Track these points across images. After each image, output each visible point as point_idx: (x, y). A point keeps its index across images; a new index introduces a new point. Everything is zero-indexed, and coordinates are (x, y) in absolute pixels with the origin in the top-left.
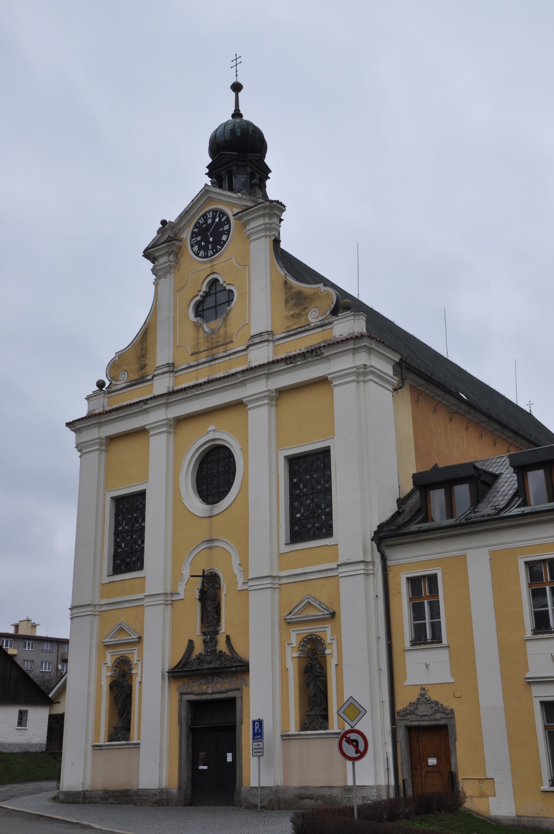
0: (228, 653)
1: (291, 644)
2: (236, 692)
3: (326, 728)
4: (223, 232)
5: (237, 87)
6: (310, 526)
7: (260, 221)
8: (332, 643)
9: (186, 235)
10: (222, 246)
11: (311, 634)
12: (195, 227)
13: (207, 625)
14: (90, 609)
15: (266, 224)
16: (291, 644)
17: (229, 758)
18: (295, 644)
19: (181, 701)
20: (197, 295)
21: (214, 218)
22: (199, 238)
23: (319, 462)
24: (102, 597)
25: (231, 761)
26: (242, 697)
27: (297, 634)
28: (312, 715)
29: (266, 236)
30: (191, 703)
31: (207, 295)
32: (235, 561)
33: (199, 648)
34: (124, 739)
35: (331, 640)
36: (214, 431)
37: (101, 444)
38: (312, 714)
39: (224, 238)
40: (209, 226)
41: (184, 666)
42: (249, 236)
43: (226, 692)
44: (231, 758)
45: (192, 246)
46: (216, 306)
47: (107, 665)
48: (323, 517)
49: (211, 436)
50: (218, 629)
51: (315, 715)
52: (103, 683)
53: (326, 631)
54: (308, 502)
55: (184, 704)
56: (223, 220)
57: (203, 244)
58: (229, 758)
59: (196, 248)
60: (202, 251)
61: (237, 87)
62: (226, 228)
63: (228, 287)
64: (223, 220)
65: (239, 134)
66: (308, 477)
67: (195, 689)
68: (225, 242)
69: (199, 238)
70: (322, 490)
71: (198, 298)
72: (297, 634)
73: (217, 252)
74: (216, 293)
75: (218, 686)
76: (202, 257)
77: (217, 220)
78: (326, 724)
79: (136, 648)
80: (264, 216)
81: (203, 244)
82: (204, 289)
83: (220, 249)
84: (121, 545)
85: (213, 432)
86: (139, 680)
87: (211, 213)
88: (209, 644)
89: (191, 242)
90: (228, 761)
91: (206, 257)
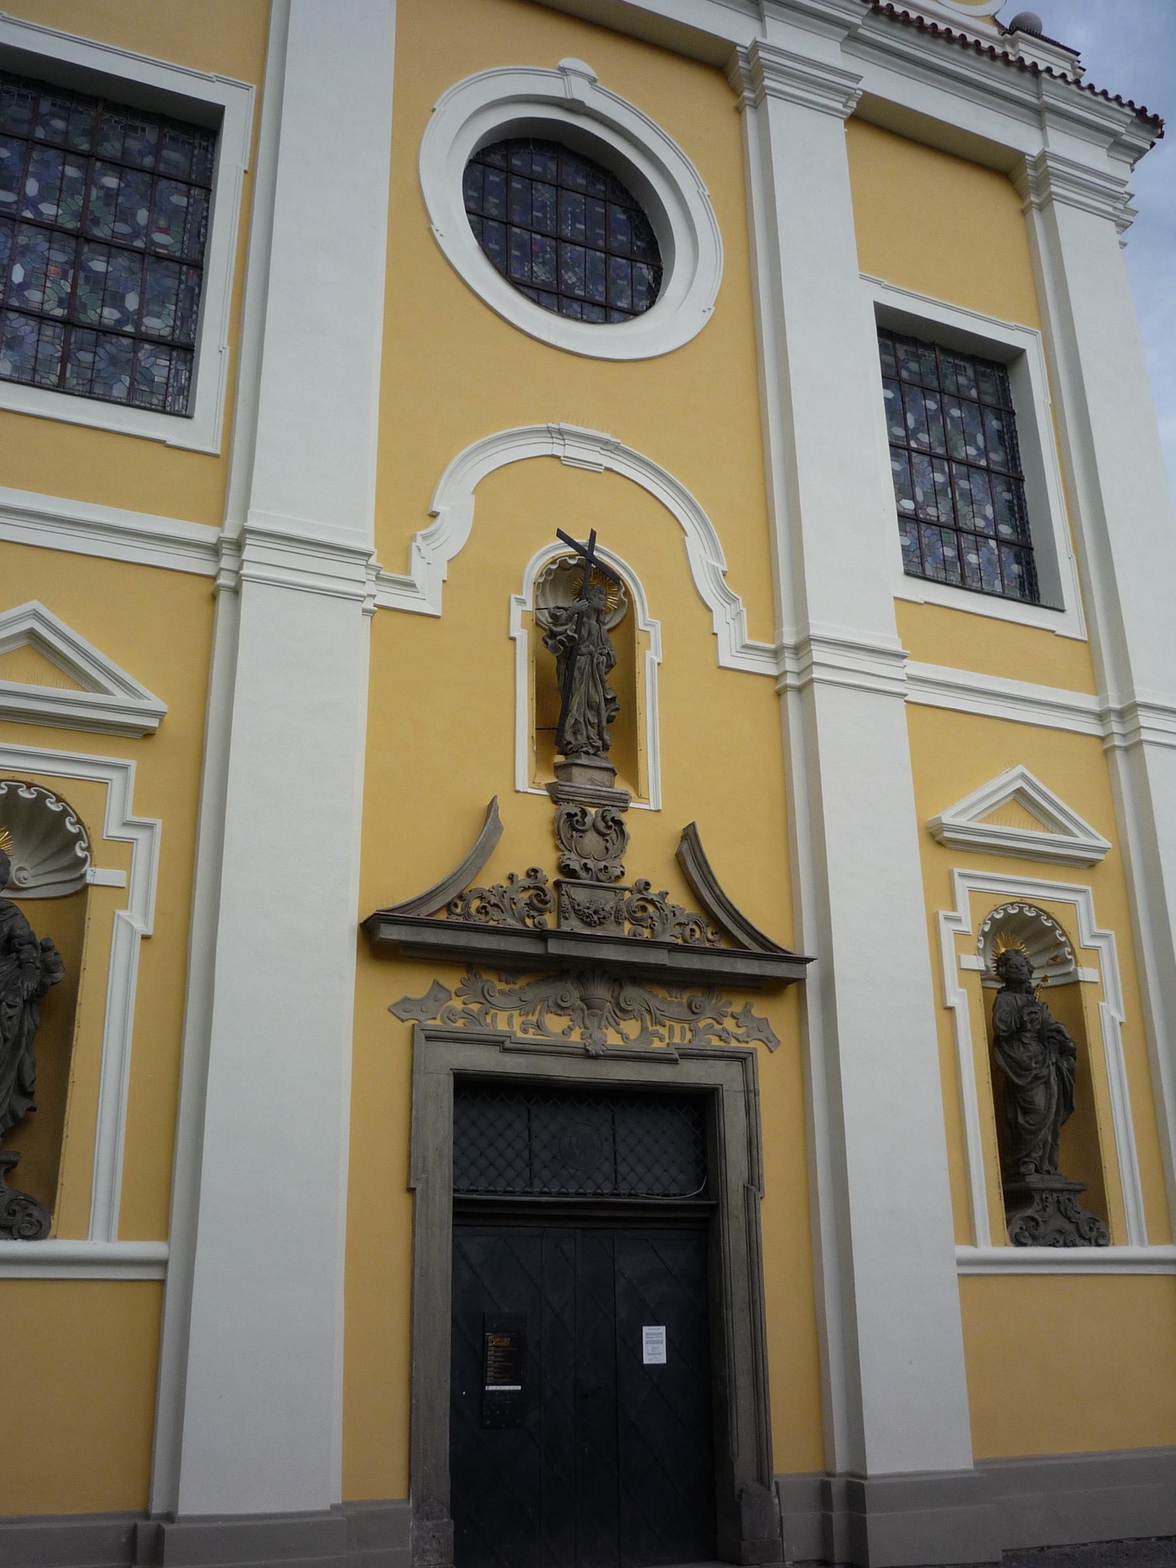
0: (678, 898)
1: (958, 920)
2: (721, 1064)
3: (1100, 1239)
8: (1096, 949)
11: (1021, 903)
13: (559, 759)
16: (958, 920)
17: (654, 1346)
18: (966, 926)
25: (662, 1359)
26: (750, 1094)
27: (972, 891)
28: (1052, 1190)
32: (704, 560)
33: (529, 845)
35: (1094, 936)
38: (1059, 1186)
41: (449, 907)
43: (674, 1062)
44: (662, 1348)
48: (993, 543)
51: (1061, 1191)
53: (1073, 904)
58: (654, 1346)
66: (932, 405)
67: (506, 1022)
72: (972, 891)
75: (632, 1028)
78: (1101, 1225)
79: (133, 764)
88: (591, 841)
90: (647, 1360)
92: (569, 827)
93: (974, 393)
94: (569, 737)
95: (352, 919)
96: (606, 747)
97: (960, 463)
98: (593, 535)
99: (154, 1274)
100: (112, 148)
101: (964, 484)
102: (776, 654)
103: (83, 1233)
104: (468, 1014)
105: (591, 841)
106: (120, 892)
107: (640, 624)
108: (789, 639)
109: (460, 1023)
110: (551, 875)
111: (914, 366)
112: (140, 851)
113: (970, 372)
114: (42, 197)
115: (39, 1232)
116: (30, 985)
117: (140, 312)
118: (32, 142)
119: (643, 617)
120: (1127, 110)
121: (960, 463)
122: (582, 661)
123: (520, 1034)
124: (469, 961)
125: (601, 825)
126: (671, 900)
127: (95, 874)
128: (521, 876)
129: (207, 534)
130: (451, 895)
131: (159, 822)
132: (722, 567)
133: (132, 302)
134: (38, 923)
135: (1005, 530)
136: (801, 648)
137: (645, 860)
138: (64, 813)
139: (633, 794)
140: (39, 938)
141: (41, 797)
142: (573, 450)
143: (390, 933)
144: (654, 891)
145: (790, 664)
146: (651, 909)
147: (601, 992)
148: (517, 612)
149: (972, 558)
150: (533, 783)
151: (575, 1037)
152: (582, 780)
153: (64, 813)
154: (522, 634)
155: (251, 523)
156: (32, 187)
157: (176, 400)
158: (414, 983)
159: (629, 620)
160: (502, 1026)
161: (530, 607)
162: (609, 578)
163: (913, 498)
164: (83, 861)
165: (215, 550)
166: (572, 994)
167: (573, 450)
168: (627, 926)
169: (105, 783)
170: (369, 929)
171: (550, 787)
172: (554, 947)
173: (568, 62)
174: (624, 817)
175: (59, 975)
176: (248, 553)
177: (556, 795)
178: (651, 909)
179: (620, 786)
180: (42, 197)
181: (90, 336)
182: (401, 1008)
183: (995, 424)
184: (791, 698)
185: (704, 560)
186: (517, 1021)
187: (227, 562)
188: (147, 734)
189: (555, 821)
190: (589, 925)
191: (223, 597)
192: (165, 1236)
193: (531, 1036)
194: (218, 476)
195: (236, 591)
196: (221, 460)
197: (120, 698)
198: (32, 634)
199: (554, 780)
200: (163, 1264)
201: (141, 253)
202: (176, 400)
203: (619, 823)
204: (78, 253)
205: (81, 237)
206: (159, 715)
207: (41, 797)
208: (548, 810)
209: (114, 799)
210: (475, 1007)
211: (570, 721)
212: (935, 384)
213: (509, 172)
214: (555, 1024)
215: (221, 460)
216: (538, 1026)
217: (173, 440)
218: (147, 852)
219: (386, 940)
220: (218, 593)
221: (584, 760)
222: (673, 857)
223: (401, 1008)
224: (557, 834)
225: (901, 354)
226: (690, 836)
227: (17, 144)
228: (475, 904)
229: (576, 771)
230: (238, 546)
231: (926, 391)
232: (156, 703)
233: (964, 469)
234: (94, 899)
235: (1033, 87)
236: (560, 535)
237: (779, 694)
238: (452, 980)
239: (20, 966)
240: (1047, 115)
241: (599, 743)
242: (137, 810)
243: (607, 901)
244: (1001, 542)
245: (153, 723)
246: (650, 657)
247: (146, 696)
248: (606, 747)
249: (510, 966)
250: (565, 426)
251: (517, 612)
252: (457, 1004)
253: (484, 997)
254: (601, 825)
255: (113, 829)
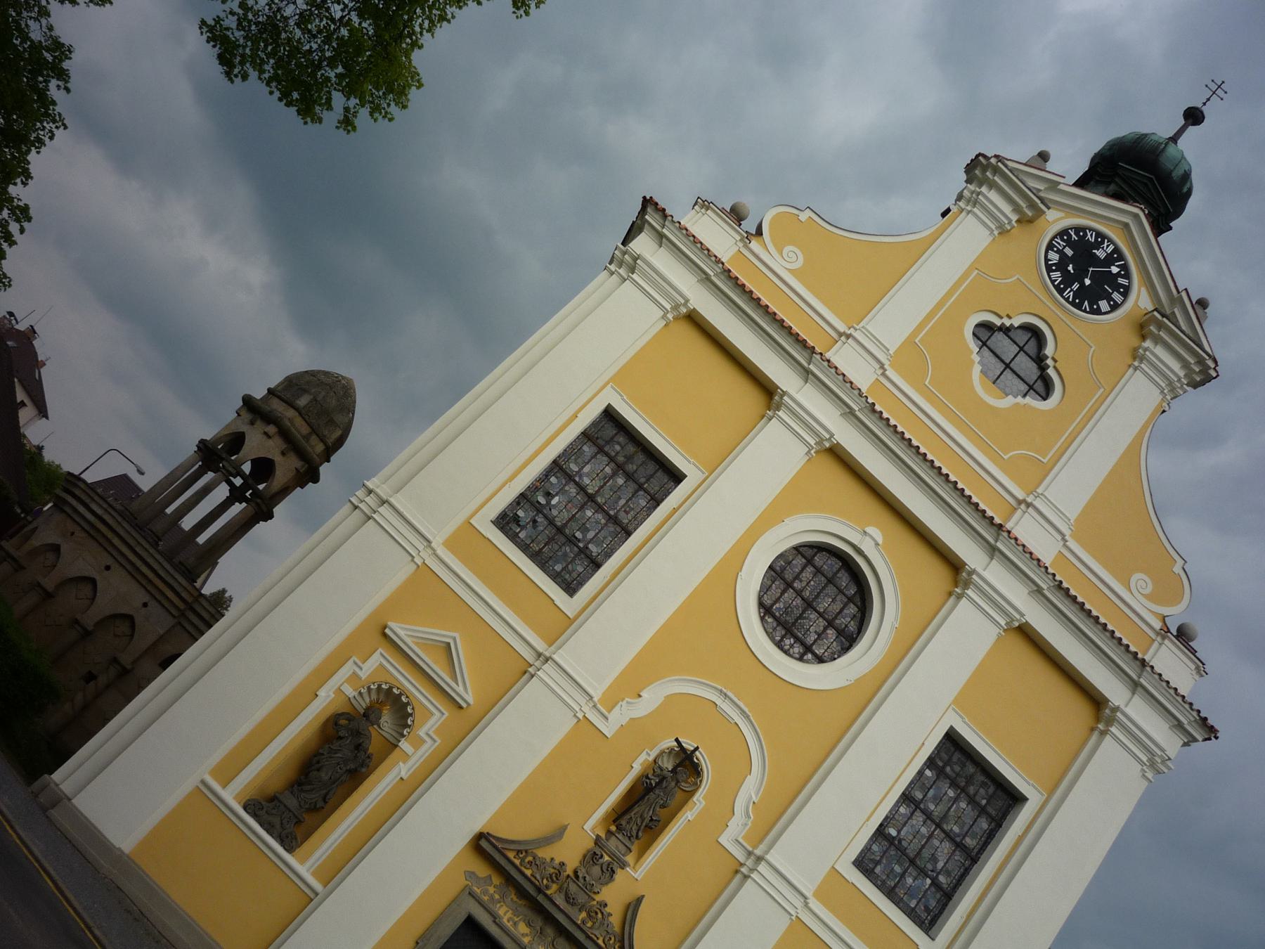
0: (615, 920)
4: (1109, 299)
5: (1194, 116)
6: (898, 869)
7: (1175, 365)
9: (1056, 221)
10: (1093, 312)
12: (1078, 229)
13: (613, 828)
14: (421, 548)
15: (1179, 380)
19: (455, 900)
20: (1001, 318)
21: (1109, 260)
22: (1069, 252)
23: (982, 791)
24: (450, 544)
29: (1162, 392)
30: (470, 923)
31: (1006, 330)
32: (750, 789)
33: (569, 853)
34: (282, 842)
36: (877, 544)
37: (676, 307)
39: (1104, 305)
40: (1096, 261)
41: (519, 852)
42: (1142, 359)
45: (1050, 247)
46: (1007, 366)
47: (357, 670)
48: (928, 881)
49: (867, 547)
50: (630, 859)
52: (322, 693)
54: (924, 830)
55: (461, 918)
56: (1121, 281)
57: (1070, 268)
59: (1054, 257)
60: (1058, 274)
61: (1194, 116)
62: (1116, 296)
63: (1051, 372)
64: (1121, 281)
65: (1185, 190)
68: (1098, 312)
69: (1069, 252)
70: (958, 839)
71: (998, 322)
73: (1079, 307)
74: (1021, 349)
76: (1053, 282)
77: (1115, 270)
79: (447, 714)
80: (1185, 365)
81: (1070, 268)
82: (1017, 322)
83: (1085, 311)
84: (553, 497)
85: (871, 541)
86: (403, 774)
87: (1111, 248)
88: (596, 870)
89: (1053, 239)
91: (1061, 292)
92: (592, 857)
93: (984, 802)
94: (624, 823)
95: (477, 827)
96: (637, 837)
97: (943, 831)
98: (697, 749)
99: (312, 896)
100: (631, 467)
101: (936, 843)
102: (750, 853)
103: (302, 862)
104: (492, 897)
105: (596, 870)
106: (406, 757)
107: (695, 799)
108: (758, 852)
109: (486, 898)
110: (569, 871)
111: (957, 768)
112: (425, 747)
113: (991, 790)
114: (588, 475)
115: (290, 850)
116: (352, 766)
117: (591, 541)
118: (601, 450)
119: (699, 797)
120: (1195, 714)
121: (943, 831)
122: (652, 796)
123: (505, 920)
124: (509, 880)
125: (605, 868)
126: (611, 919)
127: (404, 744)
128: (557, 862)
129: (540, 645)
130: (521, 847)
131: (439, 741)
132: (754, 798)
133: (591, 535)
134: (374, 747)
135: (942, 879)
136: (759, 859)
137: (613, 896)
138: (411, 715)
139: (632, 864)
140: (370, 751)
141: (408, 704)
142: (726, 706)
143: (484, 843)
144: (608, 910)
145: (750, 863)
146: (600, 915)
147: (550, 931)
148: (643, 757)
149: (909, 881)
150: (593, 830)
151: (526, 940)
152: (613, 844)
153: (411, 715)
154: (637, 768)
155: (555, 657)
156: (587, 469)
157: (571, 588)
158: (482, 870)
159: (692, 793)
160: (501, 912)
161: (651, 759)
162: (696, 771)
163: (899, 832)
164: (403, 736)
165: (539, 655)
166: (539, 923)
167: (726, 706)
168: (584, 915)
169: (432, 714)
170: (481, 836)
171: (598, 836)
172: (540, 898)
173: (868, 530)
174: (619, 871)
175: (364, 770)
176: (546, 667)
177: (598, 841)
178: (600, 915)
179: (630, 859)
180: (588, 475)
181: (563, 539)
182: (470, 875)
183: (985, 826)
184: (739, 876)
185: (750, 789)
186: (509, 915)
187: (537, 664)
188: (461, 707)
189: (588, 851)
190: (568, 902)
191: (527, 675)
192: (325, 886)
193: (509, 925)
194: (559, 629)
195: (532, 676)
196: (571, 621)
197: (460, 689)
198: (449, 644)
199: (603, 836)
200: (317, 894)
201: (610, 517)
202: (571, 588)
203: (613, 872)
204: (585, 504)
205: (591, 498)
206: (468, 704)
207: (408, 704)
208: (591, 844)
209: (431, 721)
210: (497, 897)
211: (628, 817)
212: (963, 784)
213: (810, 562)
214: (523, 928)
215: (571, 621)
216: (515, 924)
217: (558, 602)
218: (427, 748)
219: (483, 845)
220: (525, 672)
221: (620, 836)
222: (627, 901)
223: (470, 875)
224: (585, 856)
225: (955, 759)
226: (639, 900)
227: (595, 449)
228: (530, 858)
229: (613, 838)
230: (547, 660)
231: (954, 784)
232: (471, 700)
233: (943, 835)
234: (397, 751)
235: (1138, 670)
236: (677, 740)
237: (737, 872)
238: (497, 880)
239: (356, 757)
240: (1139, 689)
241: (634, 833)
242: (436, 732)
243: (582, 898)
244: (935, 883)
245: (464, 705)
246: (688, 815)
247: (468, 693)
248: (637, 837)
249: (522, 893)
250: (729, 694)
251: (643, 757)
252: (491, 890)
253: (503, 897)
254: (605, 868)
255: (422, 733)
